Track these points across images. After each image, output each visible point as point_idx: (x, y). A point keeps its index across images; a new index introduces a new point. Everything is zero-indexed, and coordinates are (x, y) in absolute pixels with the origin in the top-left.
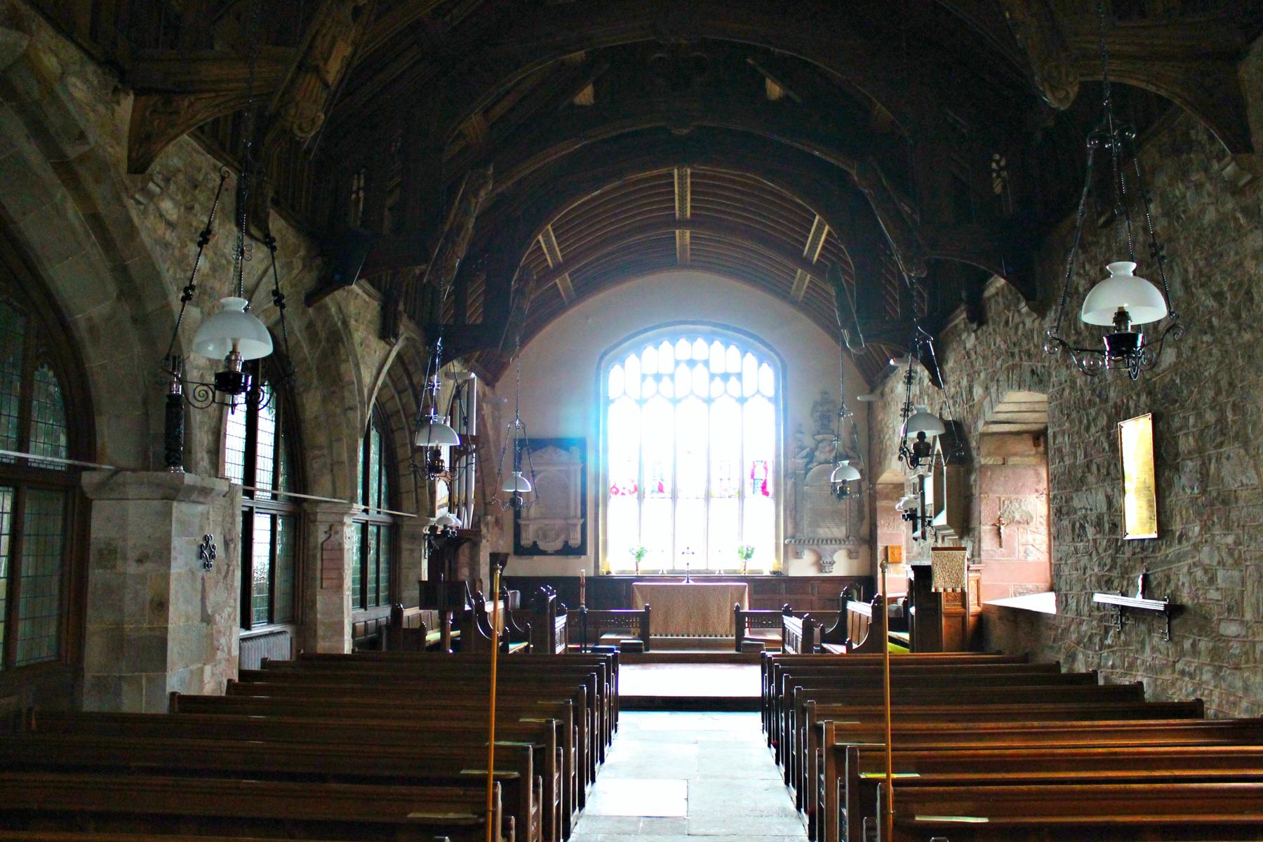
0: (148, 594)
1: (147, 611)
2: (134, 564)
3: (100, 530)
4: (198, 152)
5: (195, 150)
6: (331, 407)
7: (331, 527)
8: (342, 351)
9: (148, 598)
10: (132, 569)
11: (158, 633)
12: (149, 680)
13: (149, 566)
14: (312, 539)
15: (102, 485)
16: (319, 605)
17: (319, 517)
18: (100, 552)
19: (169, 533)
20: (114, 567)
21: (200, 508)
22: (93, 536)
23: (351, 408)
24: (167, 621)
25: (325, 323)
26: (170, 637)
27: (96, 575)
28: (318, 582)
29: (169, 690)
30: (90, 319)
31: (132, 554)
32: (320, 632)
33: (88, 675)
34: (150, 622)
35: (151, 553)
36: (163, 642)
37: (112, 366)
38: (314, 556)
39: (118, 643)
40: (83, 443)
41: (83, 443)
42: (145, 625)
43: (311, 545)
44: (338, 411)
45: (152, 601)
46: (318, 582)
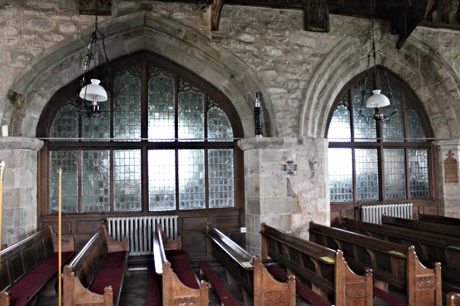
0: (254, 185)
1: (254, 191)
4: (267, 11)
5: (264, 11)
6: (438, 93)
7: (450, 151)
8: (436, 64)
12: (256, 217)
13: (254, 174)
14: (440, 159)
16: (445, 191)
17: (442, 147)
19: (258, 161)
21: (282, 150)
23: (452, 91)
24: (259, 195)
25: (417, 53)
26: (260, 201)
28: (444, 180)
29: (261, 222)
30: (224, 87)
31: (249, 170)
32: (446, 204)
35: (254, 169)
36: (259, 203)
37: (237, 101)
38: (441, 167)
42: (254, 197)
43: (440, 162)
44: (443, 93)
46: (444, 180)
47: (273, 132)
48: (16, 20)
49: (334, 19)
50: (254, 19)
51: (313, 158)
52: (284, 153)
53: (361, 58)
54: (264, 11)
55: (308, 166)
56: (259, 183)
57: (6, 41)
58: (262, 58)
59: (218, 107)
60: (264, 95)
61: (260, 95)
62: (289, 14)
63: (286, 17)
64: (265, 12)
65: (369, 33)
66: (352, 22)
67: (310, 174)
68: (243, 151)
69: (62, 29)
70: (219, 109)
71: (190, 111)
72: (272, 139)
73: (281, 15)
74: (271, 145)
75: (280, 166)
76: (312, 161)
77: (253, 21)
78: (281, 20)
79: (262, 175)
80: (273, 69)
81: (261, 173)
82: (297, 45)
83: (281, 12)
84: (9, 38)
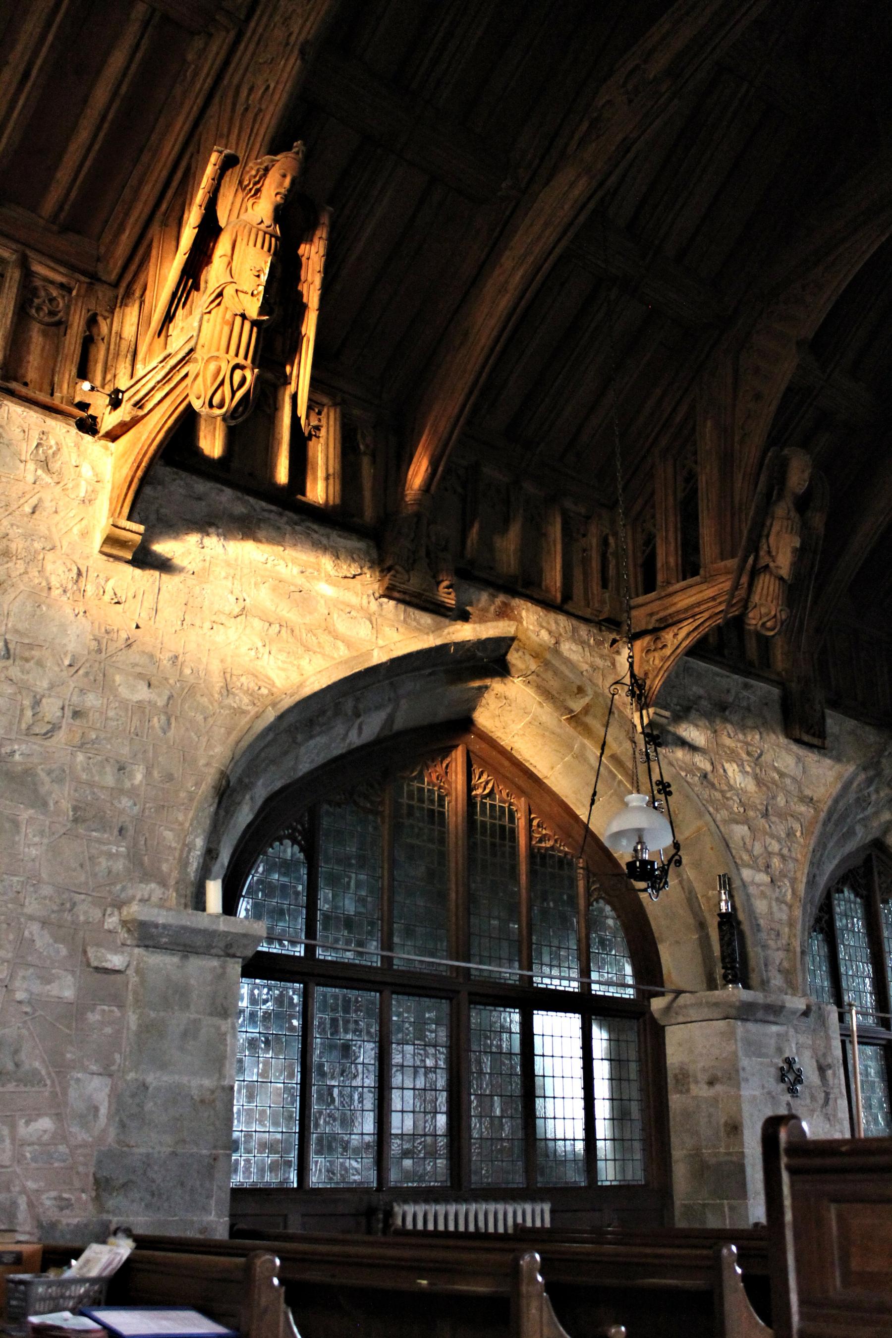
1: (722, 1134)
2: (706, 1087)
3: (674, 1055)
5: (718, 675)
9: (722, 1121)
10: (701, 1091)
11: (735, 1159)
12: (732, 1208)
13: (719, 1088)
15: (668, 1009)
18: (676, 1076)
20: (688, 1091)
21: (774, 1028)
22: (668, 1062)
24: (742, 1144)
27: (675, 1100)
31: (703, 1077)
33: (678, 1203)
34: (727, 1147)
35: (719, 1074)
39: (701, 1169)
40: (649, 973)
41: (649, 973)
42: (722, 1150)
45: (726, 1124)
47: (754, 978)
48: (232, 572)
49: (834, 723)
50: (701, 692)
51: (824, 1055)
52: (778, 1035)
53: (859, 817)
54: (718, 675)
55: (817, 1073)
56: (740, 1110)
57: (207, 625)
58: (723, 792)
59: (608, 902)
60: (736, 884)
61: (726, 882)
62: (759, 693)
63: (753, 698)
64: (718, 679)
65: (879, 762)
66: (852, 733)
67: (823, 1095)
68: (664, 1027)
69: (341, 625)
70: (608, 908)
71: (551, 904)
72: (766, 997)
73: (745, 693)
74: (760, 1015)
75: (773, 1070)
76: (822, 1061)
77: (700, 697)
78: (745, 704)
79: (746, 1092)
80: (743, 823)
81: (743, 1085)
82: (776, 769)
83: (746, 686)
84: (214, 618)
